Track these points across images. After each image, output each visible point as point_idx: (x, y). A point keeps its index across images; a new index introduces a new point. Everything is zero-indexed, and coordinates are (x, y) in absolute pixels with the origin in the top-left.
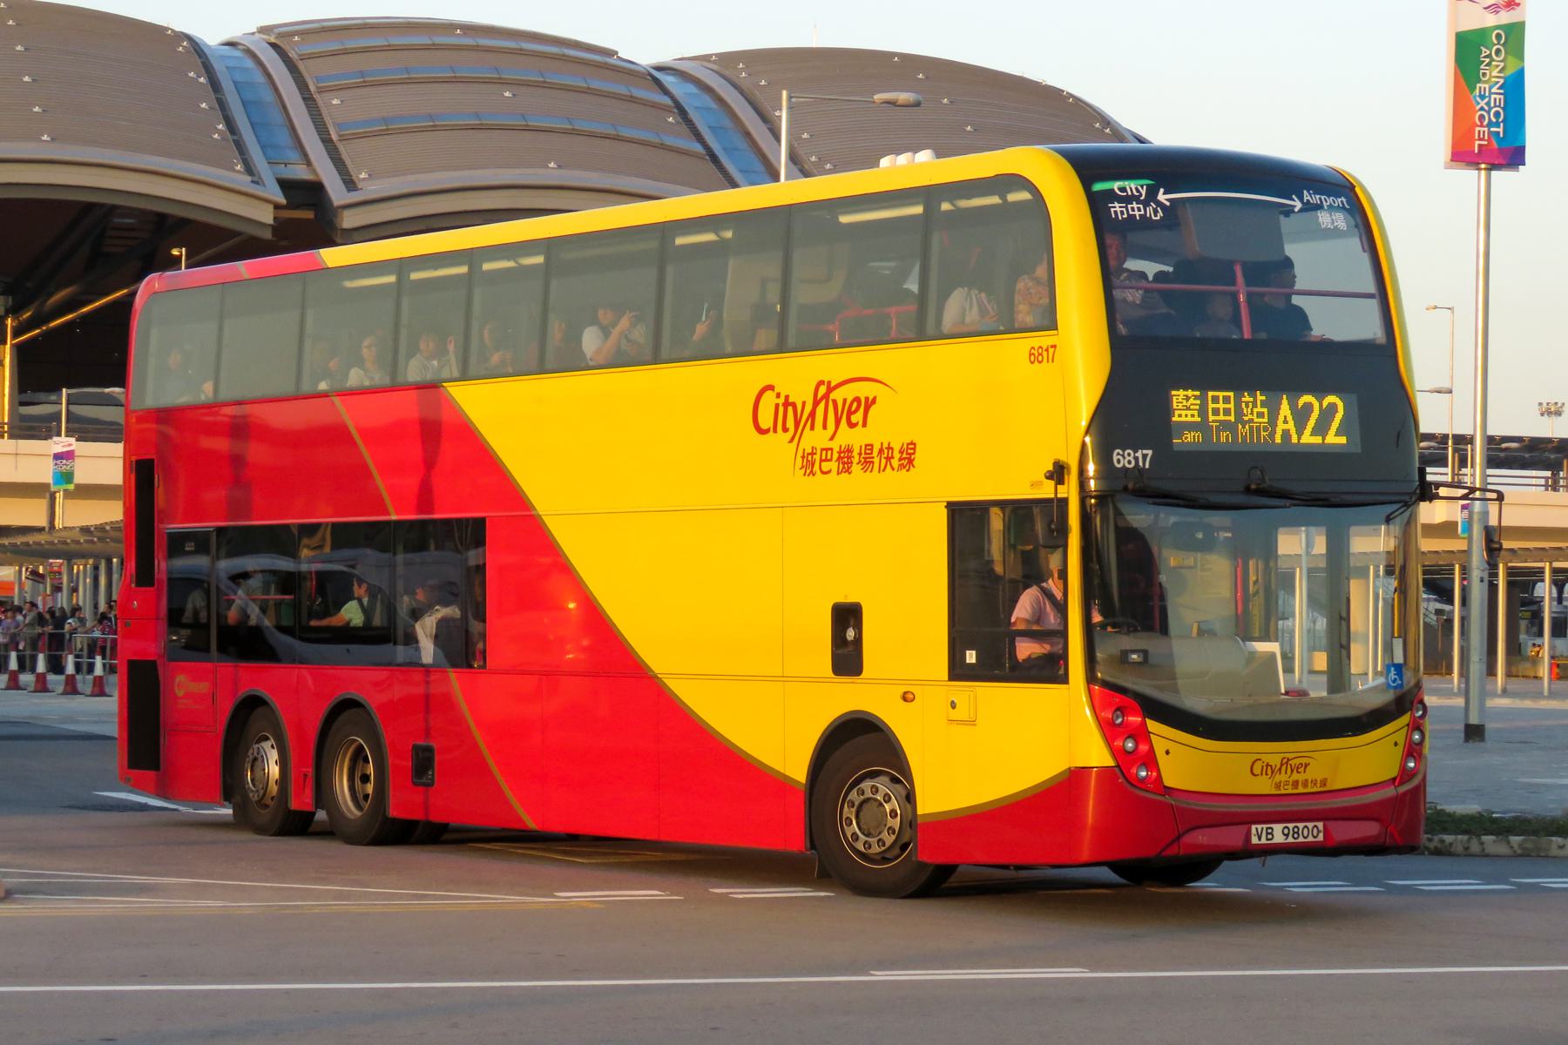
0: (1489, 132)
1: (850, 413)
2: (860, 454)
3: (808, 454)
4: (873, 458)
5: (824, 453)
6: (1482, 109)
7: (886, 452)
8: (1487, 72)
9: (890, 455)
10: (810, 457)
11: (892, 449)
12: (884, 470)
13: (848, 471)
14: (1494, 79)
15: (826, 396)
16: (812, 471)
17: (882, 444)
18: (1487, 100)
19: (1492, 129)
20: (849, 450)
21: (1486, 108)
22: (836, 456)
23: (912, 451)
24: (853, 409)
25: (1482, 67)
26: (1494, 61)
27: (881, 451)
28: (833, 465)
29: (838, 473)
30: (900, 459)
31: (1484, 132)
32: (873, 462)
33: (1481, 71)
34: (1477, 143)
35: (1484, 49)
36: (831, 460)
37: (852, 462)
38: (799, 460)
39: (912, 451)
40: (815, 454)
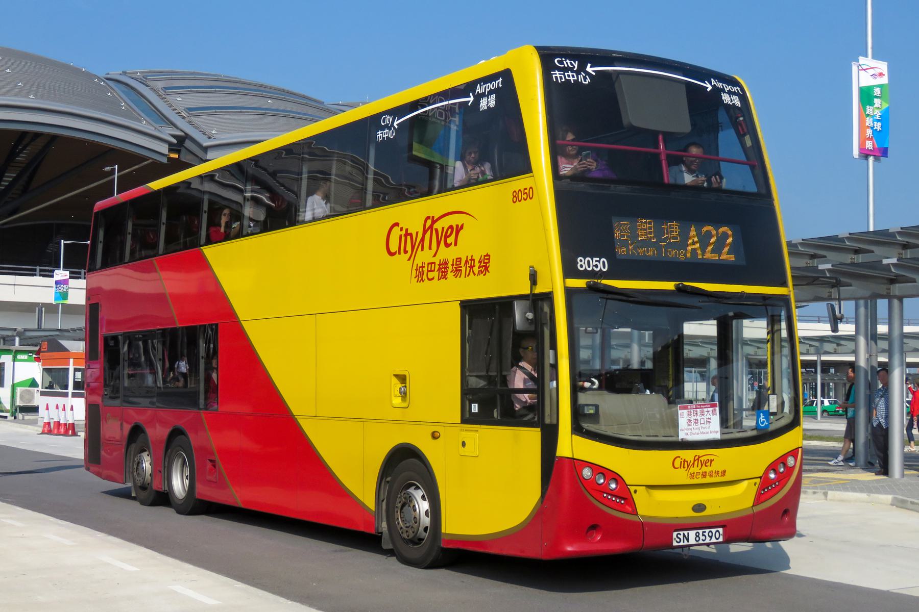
1: (447, 237)
2: (453, 265)
3: (420, 267)
4: (461, 267)
5: (430, 265)
7: (470, 262)
9: (472, 265)
10: (421, 269)
11: (474, 260)
12: (468, 276)
13: (445, 278)
15: (431, 227)
16: (422, 279)
17: (467, 257)
20: (446, 263)
22: (437, 267)
23: (486, 261)
24: (448, 234)
27: (466, 262)
28: (435, 274)
29: (439, 279)
30: (479, 267)
32: (461, 270)
36: (434, 271)
37: (447, 271)
38: (414, 272)
39: (487, 261)
40: (424, 267)
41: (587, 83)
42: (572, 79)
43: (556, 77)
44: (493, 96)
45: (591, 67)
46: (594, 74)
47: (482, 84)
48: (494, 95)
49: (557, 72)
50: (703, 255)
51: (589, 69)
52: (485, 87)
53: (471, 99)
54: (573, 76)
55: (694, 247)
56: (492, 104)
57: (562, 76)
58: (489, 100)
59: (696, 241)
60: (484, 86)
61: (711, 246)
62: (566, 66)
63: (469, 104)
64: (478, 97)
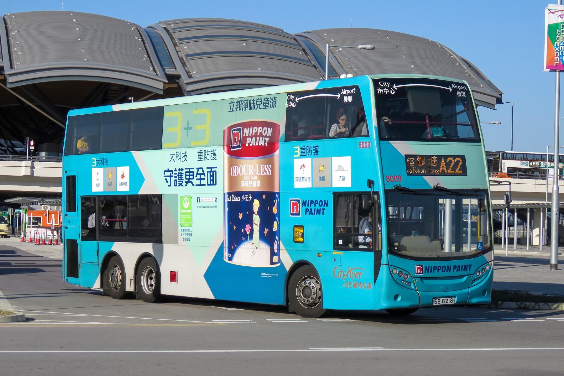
0: (559, 58)
6: (557, 51)
8: (559, 38)
14: (561, 41)
18: (559, 48)
19: (561, 58)
21: (559, 51)
25: (557, 36)
26: (561, 34)
31: (558, 59)
33: (557, 38)
34: (555, 63)
35: (558, 30)
41: (393, 93)
42: (386, 92)
43: (379, 92)
44: (351, 97)
45: (395, 86)
46: (397, 89)
47: (345, 89)
48: (351, 96)
49: (380, 89)
50: (447, 172)
51: (395, 87)
52: (346, 92)
53: (339, 96)
54: (387, 91)
55: (443, 168)
56: (350, 100)
57: (382, 91)
58: (348, 98)
59: (444, 165)
60: (346, 91)
61: (451, 167)
62: (384, 85)
63: (338, 98)
64: (343, 96)
